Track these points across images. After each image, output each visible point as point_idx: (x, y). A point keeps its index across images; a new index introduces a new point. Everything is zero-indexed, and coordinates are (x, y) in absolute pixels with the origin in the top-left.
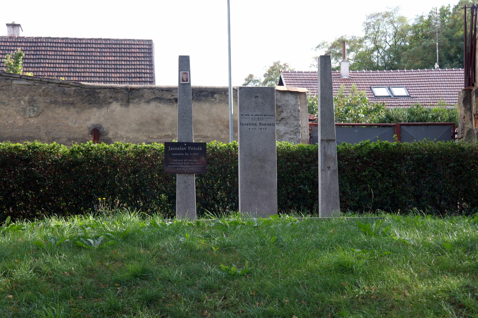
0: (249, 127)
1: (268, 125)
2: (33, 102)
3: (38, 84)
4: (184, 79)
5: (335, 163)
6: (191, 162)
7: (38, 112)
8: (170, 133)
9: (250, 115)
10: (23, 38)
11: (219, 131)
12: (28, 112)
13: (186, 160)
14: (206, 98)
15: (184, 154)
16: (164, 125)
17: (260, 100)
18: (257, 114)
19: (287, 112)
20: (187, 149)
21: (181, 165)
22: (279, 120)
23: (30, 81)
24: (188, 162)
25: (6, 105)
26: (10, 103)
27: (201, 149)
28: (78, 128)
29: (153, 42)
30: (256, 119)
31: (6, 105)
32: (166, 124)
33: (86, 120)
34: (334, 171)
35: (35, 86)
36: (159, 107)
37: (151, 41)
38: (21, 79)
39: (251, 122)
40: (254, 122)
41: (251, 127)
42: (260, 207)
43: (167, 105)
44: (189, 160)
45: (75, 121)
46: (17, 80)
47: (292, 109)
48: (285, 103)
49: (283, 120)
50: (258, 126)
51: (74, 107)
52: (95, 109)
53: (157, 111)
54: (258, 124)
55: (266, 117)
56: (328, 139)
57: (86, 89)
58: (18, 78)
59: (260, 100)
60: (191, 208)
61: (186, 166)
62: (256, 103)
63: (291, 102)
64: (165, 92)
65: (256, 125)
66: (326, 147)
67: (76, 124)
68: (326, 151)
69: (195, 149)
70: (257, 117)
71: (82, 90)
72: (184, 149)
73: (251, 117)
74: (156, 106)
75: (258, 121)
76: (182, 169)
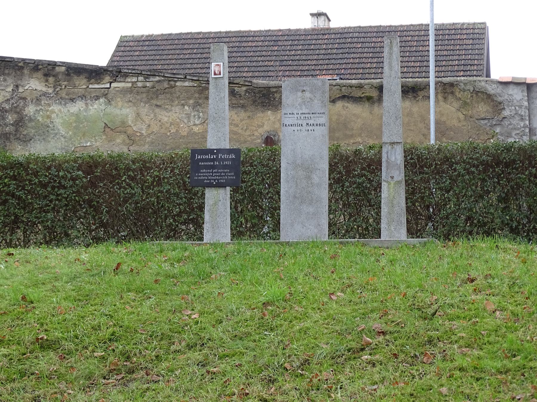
0: (293, 128)
1: (317, 125)
2: (198, 107)
3: (204, 85)
4: (216, 72)
5: (400, 172)
6: (221, 173)
7: (204, 118)
8: (360, 140)
9: (295, 114)
10: (333, 29)
11: (422, 136)
12: (192, 119)
13: (216, 170)
14: (406, 94)
15: (214, 163)
16: (352, 129)
17: (308, 95)
18: (304, 112)
19: (510, 109)
20: (217, 157)
21: (210, 176)
22: (500, 119)
23: (195, 82)
24: (218, 172)
25: (168, 111)
26: (173, 108)
27: (234, 157)
28: (250, 136)
29: (487, 25)
30: (302, 118)
31: (168, 111)
32: (355, 128)
33: (259, 126)
34: (399, 182)
35: (201, 88)
36: (347, 108)
37: (484, 23)
38: (185, 80)
39: (296, 122)
40: (300, 122)
41: (296, 128)
42: (304, 227)
43: (356, 105)
44: (219, 171)
45: (245, 128)
46: (181, 81)
47: (517, 106)
48: (508, 99)
49: (506, 119)
50: (305, 127)
51: (245, 111)
52: (269, 112)
53: (344, 112)
54: (304, 124)
55: (315, 115)
56: (392, 141)
57: (259, 89)
58: (183, 78)
59: (308, 95)
60: (222, 229)
61: (216, 178)
62: (303, 99)
63: (515, 96)
64: (354, 88)
65: (302, 125)
66: (389, 152)
67: (247, 131)
68: (389, 157)
69: (227, 157)
70: (304, 115)
71: (255, 90)
72: (214, 157)
73: (296, 116)
74: (343, 106)
75: (305, 121)
76: (210, 181)
